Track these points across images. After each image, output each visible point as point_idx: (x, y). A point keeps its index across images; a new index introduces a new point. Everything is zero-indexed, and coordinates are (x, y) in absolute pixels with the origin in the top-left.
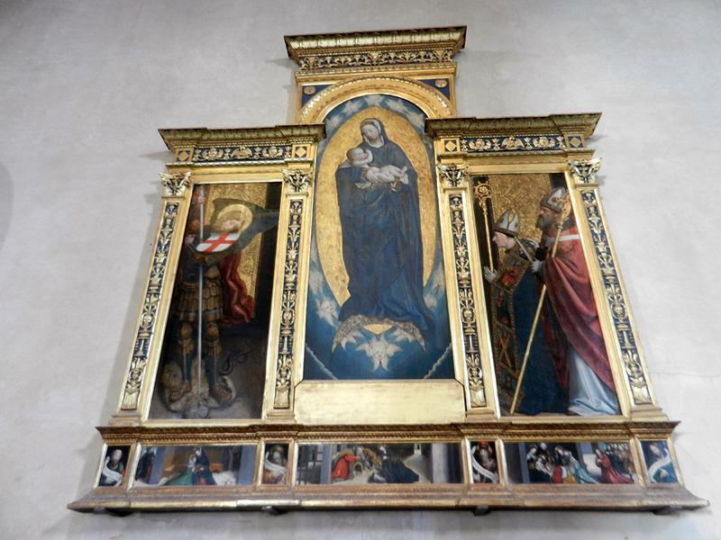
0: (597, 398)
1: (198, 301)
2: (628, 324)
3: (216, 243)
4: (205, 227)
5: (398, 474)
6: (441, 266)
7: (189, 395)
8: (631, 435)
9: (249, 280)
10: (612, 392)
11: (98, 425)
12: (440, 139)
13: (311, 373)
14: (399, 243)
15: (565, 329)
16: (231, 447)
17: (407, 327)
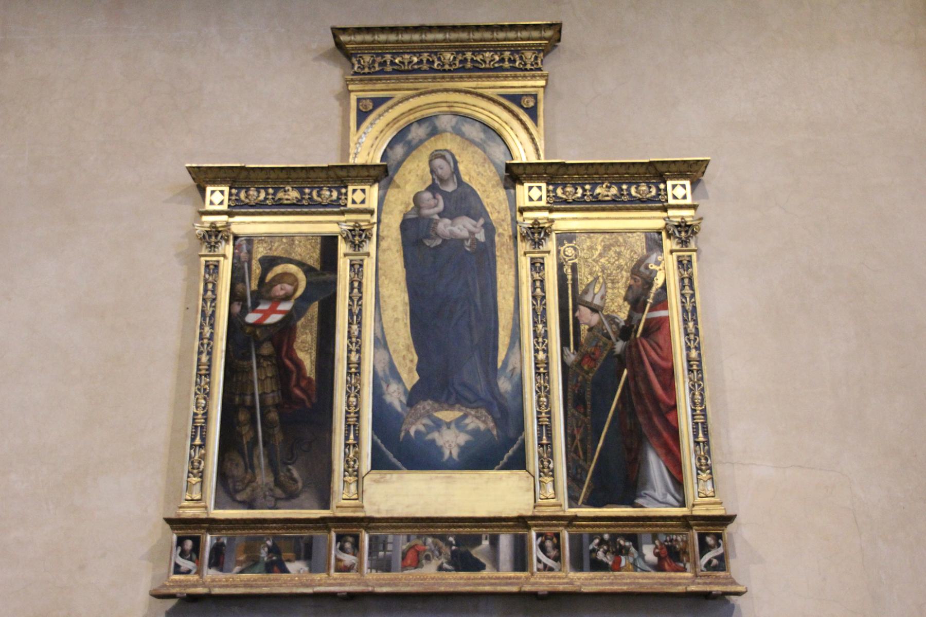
0: (664, 491)
1: (252, 382)
2: (705, 415)
3: (266, 314)
4: (252, 293)
5: (463, 561)
6: (517, 344)
7: (254, 484)
8: (689, 527)
9: (307, 359)
10: (679, 483)
11: (167, 516)
12: (522, 184)
13: (379, 463)
14: (473, 318)
15: (641, 419)
16: (302, 537)
17: (479, 415)
